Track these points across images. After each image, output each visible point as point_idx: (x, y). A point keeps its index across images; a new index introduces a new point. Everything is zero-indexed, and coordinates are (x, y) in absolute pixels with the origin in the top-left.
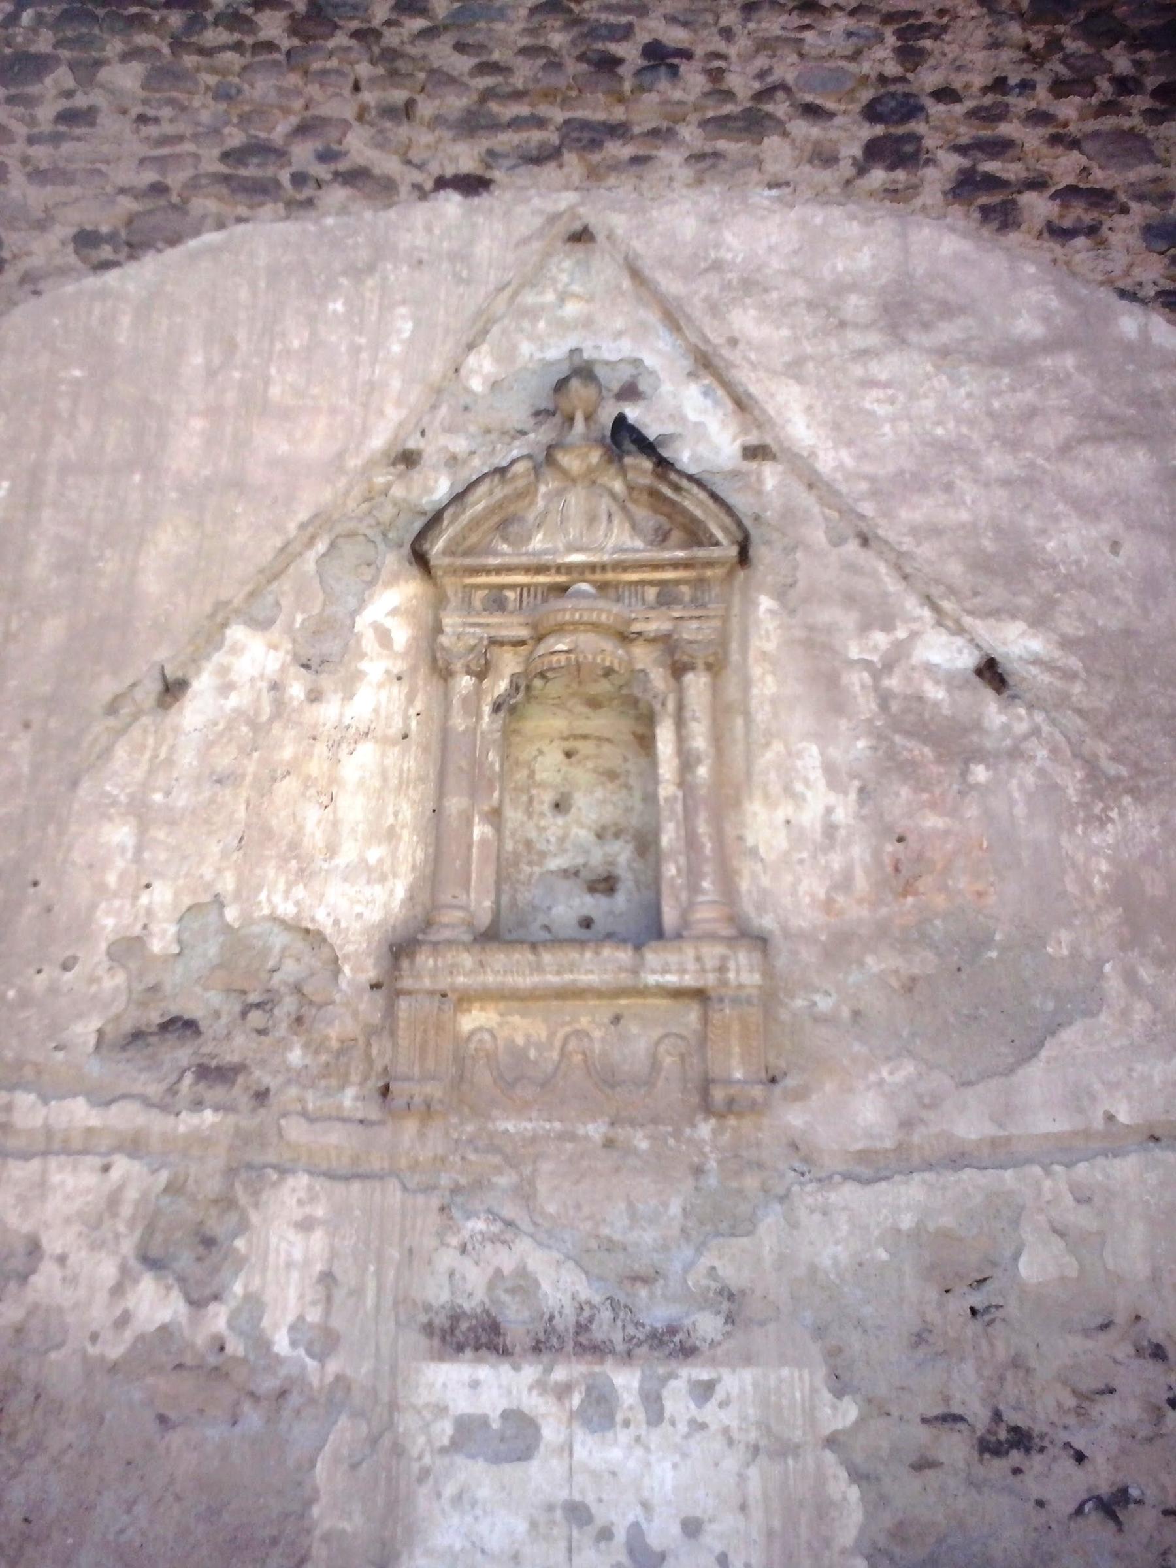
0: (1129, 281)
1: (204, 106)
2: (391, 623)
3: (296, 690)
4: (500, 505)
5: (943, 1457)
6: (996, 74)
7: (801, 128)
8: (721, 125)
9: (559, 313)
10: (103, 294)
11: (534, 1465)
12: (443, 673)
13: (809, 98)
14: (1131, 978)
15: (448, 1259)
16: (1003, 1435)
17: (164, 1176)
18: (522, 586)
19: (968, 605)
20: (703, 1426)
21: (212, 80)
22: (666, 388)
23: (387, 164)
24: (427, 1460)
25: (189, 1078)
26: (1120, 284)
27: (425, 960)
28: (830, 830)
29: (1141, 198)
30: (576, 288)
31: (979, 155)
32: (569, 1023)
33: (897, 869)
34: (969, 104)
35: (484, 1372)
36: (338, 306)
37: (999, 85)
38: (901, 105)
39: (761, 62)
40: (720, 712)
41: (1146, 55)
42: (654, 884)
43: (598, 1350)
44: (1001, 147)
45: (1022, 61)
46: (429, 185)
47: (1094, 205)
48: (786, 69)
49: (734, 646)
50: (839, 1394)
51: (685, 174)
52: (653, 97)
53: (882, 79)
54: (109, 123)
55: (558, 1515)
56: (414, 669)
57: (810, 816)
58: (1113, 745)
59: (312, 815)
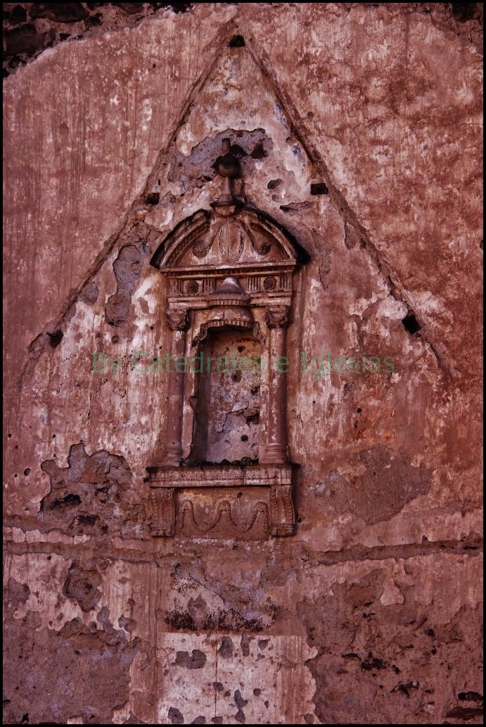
2: (146, 298)
3: (108, 337)
5: (348, 669)
9: (226, 98)
11: (204, 670)
14: (443, 478)
17: (70, 562)
19: (406, 283)
20: (263, 657)
22: (276, 149)
24: (168, 667)
25: (76, 522)
28: (331, 406)
30: (233, 81)
32: (221, 498)
33: (356, 426)
35: (186, 636)
36: (115, 101)
43: (227, 629)
49: (297, 310)
50: (311, 646)
55: (212, 687)
56: (159, 323)
57: (323, 400)
58: (458, 361)
59: (118, 401)
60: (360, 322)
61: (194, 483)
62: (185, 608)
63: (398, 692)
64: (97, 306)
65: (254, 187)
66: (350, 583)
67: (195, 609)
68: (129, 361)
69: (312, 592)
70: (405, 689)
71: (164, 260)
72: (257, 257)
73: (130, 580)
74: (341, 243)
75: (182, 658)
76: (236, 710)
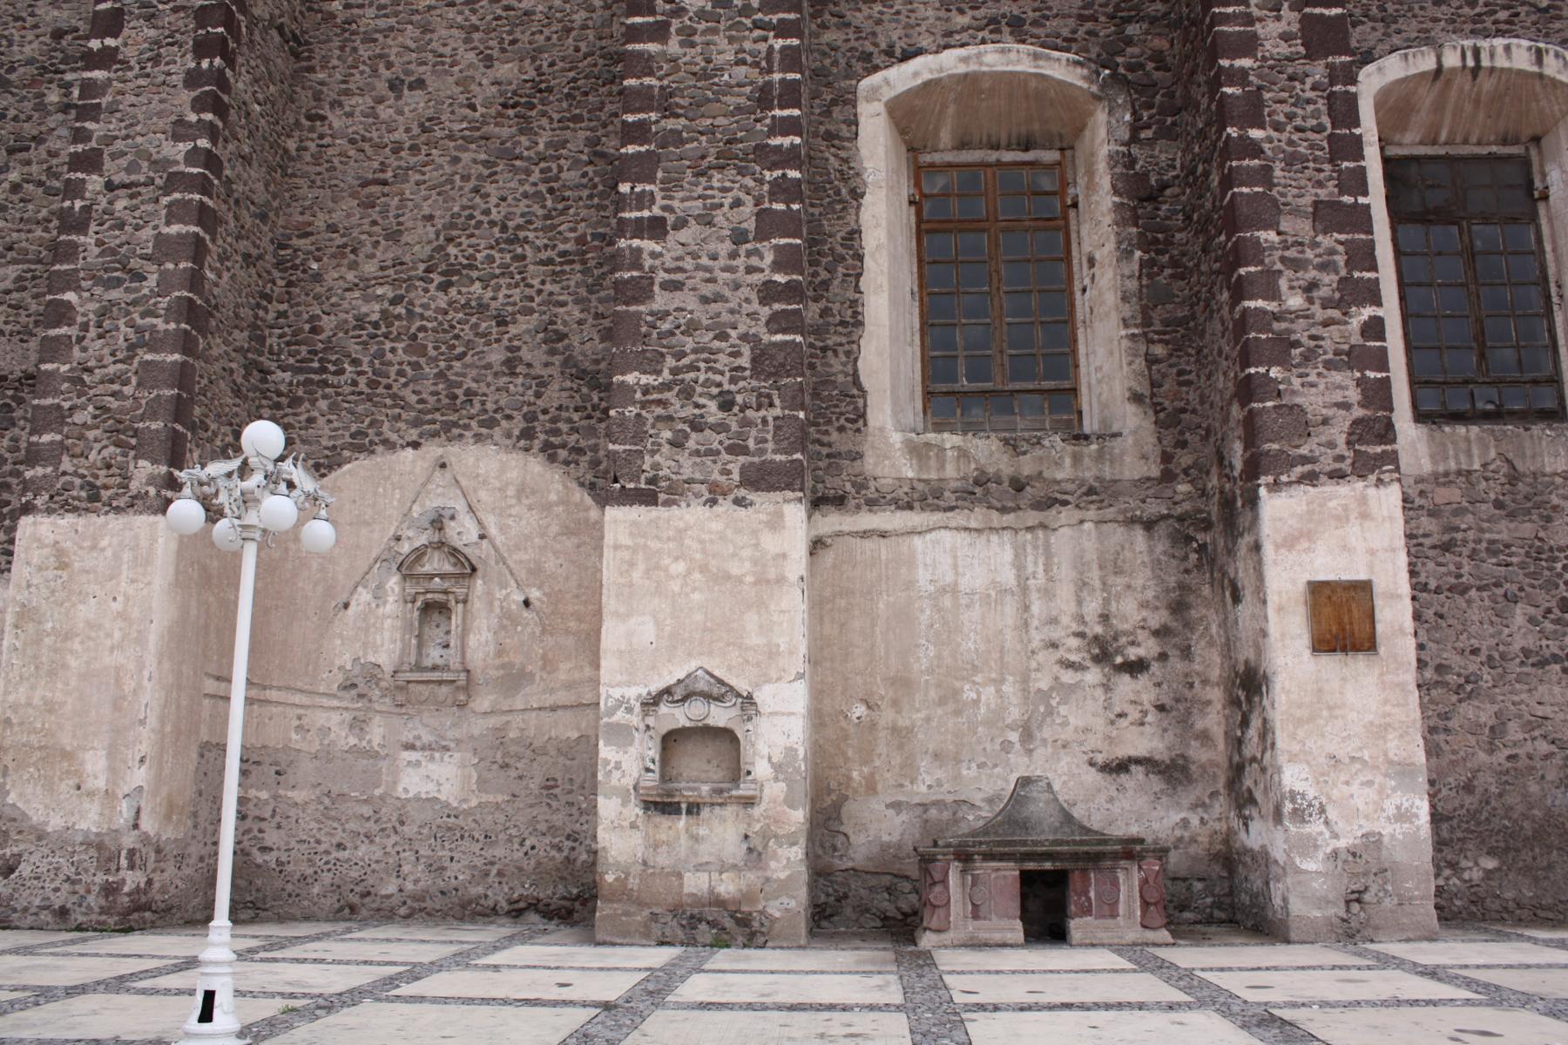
7: (504, 423)
8: (482, 424)
13: (508, 412)
23: (394, 437)
37: (560, 408)
44: (557, 432)
48: (502, 403)
51: (471, 441)
53: (530, 404)
54: (321, 421)
57: (483, 639)
69: (476, 732)
70: (520, 778)
74: (493, 563)
75: (409, 763)
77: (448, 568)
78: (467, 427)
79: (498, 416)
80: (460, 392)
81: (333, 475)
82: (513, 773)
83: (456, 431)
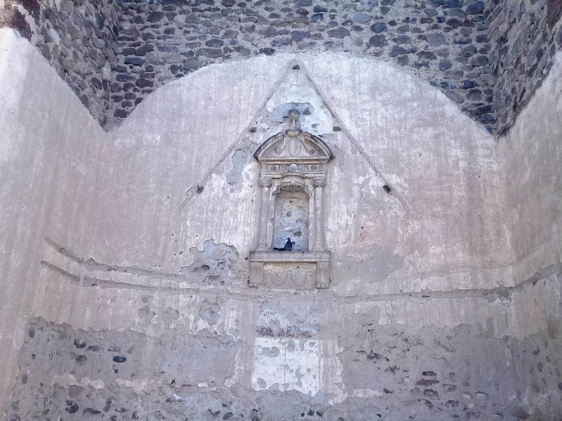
0: (434, 79)
1: (201, 28)
2: (249, 173)
3: (228, 190)
4: (274, 144)
5: (360, 359)
6: (407, 16)
7: (354, 33)
8: (332, 34)
9: (290, 90)
10: (179, 85)
11: (278, 358)
12: (262, 186)
13: (357, 24)
15: (261, 317)
16: (373, 355)
17: (203, 299)
18: (279, 164)
19: (383, 170)
20: (312, 351)
21: (203, 19)
22: (316, 110)
23: (248, 45)
26: (432, 80)
27: (257, 255)
28: (347, 225)
29: (440, 55)
30: (294, 83)
31: (400, 42)
32: (288, 268)
33: (361, 235)
34: (398, 26)
35: (268, 339)
37: (407, 20)
38: (381, 26)
39: (345, 13)
40: (324, 196)
41: (447, 10)
42: (307, 234)
43: (292, 336)
44: (405, 40)
45: (414, 12)
46: (258, 51)
47: (428, 57)
48: (351, 16)
49: (328, 180)
50: (340, 346)
51: (323, 48)
52: (315, 24)
53: (377, 18)
54: (178, 33)
55: (283, 367)
56: (255, 184)
57: (343, 222)
58: (413, 206)
60: (361, 186)
61: (275, 260)
62: (268, 324)
63: (389, 371)
64: (224, 176)
65: (305, 126)
66: (361, 313)
67: (273, 325)
68: (236, 203)
70: (393, 370)
71: (261, 154)
72: (307, 154)
73: (236, 309)
75: (265, 350)
76: (297, 380)
77: (304, 154)
78: (318, 36)
79: (348, 28)
80: (310, 9)
81: (190, 76)
82: (384, 365)
83: (307, 41)
